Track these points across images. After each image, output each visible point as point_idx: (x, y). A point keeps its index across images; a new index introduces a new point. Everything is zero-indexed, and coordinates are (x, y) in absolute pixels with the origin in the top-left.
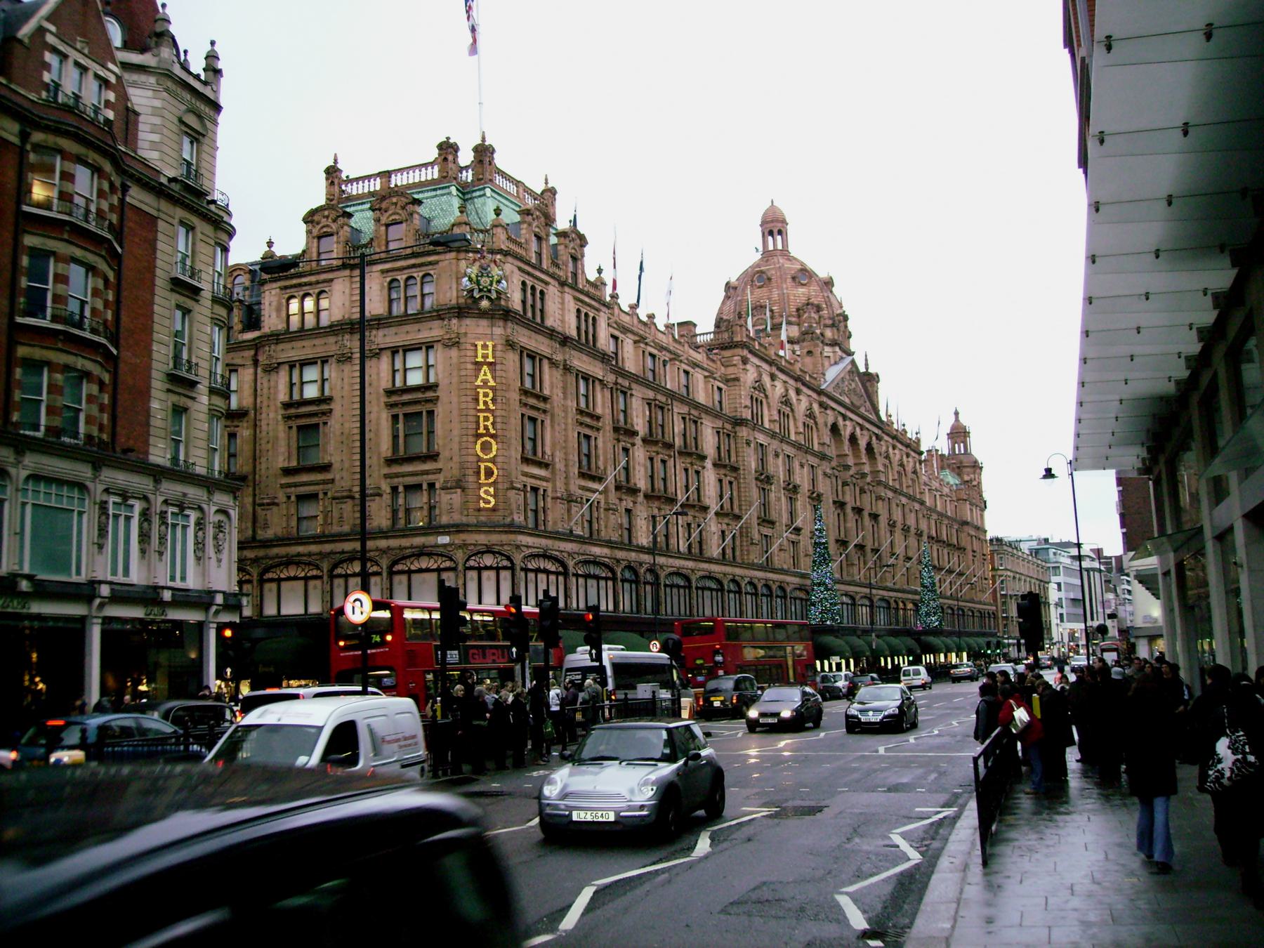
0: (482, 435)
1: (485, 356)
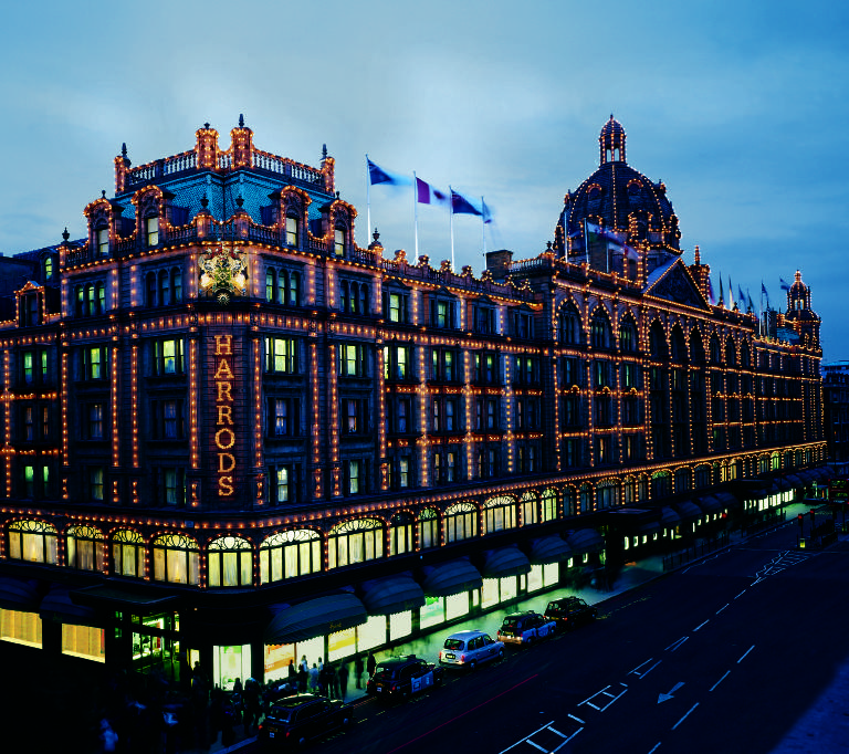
0: (221, 427)
1: (224, 349)
